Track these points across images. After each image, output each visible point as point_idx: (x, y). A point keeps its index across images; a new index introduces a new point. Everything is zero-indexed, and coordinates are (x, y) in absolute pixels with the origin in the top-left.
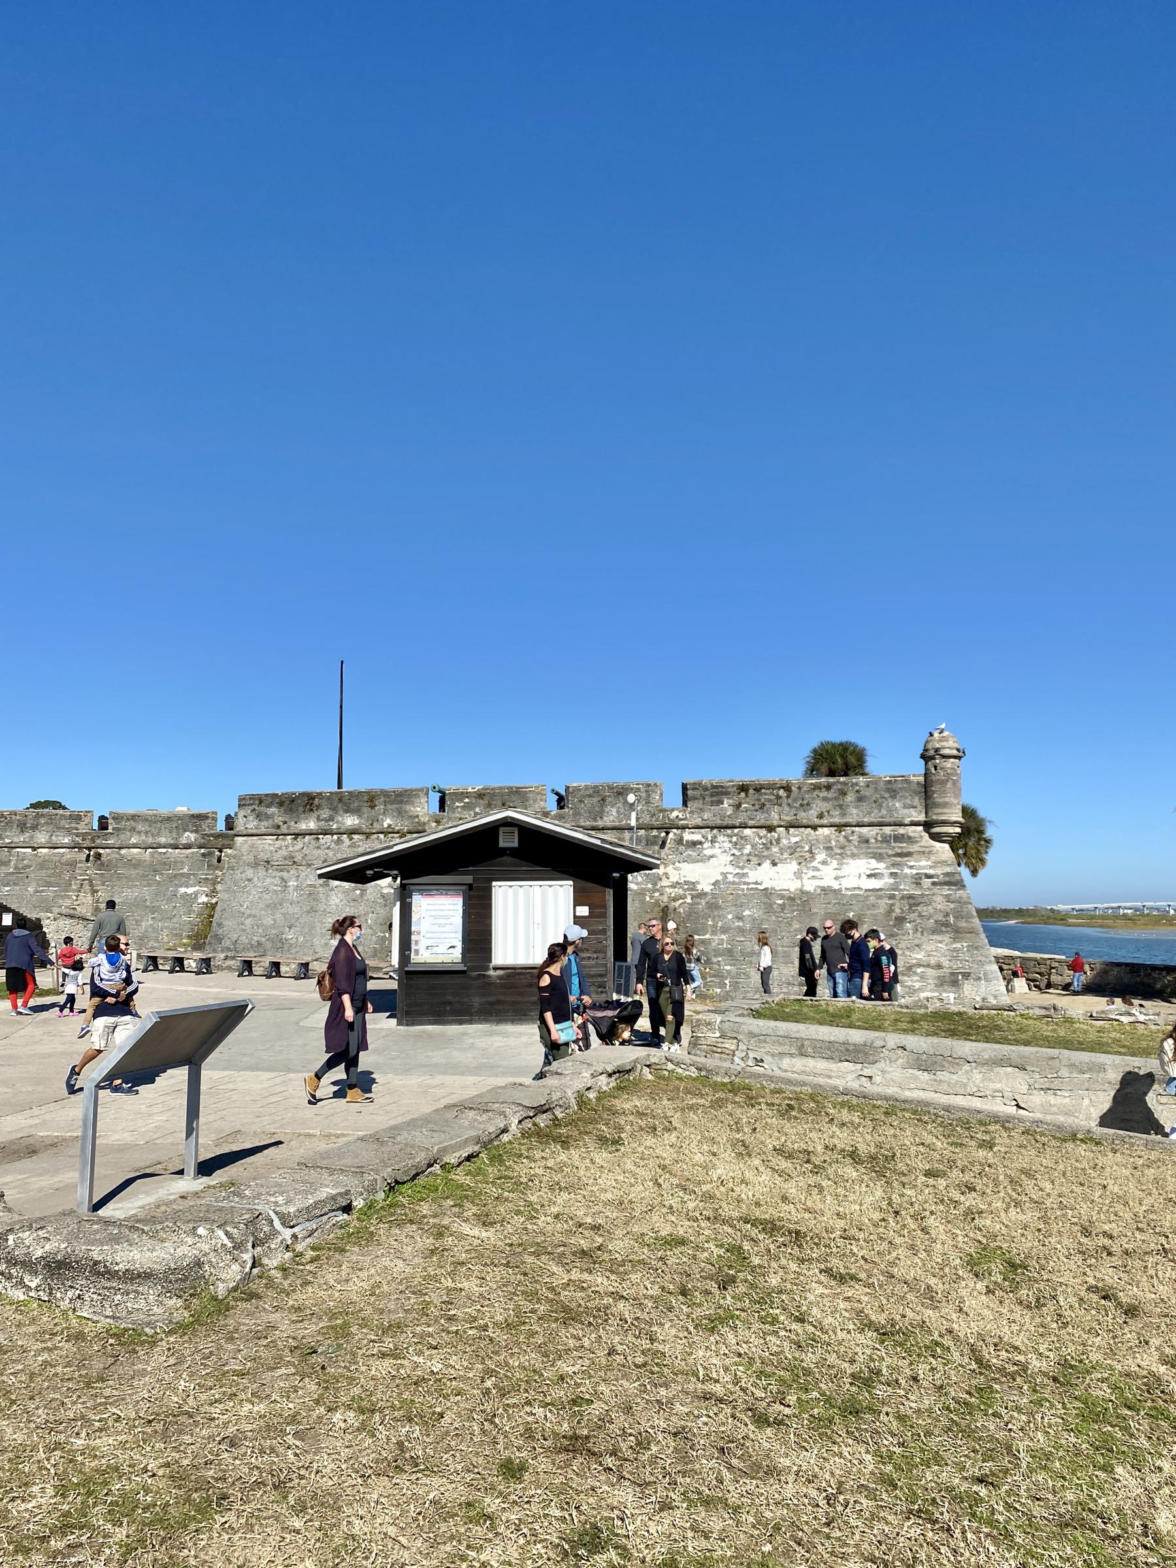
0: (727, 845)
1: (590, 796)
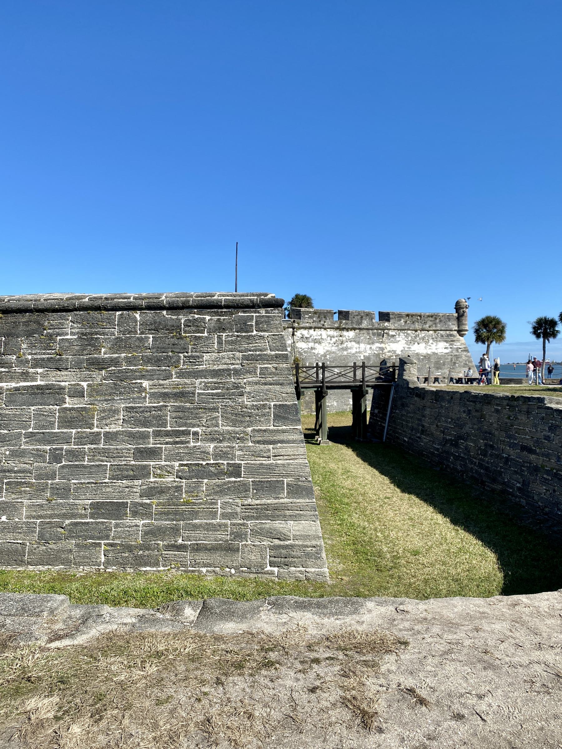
0: (404, 337)
1: (357, 315)
